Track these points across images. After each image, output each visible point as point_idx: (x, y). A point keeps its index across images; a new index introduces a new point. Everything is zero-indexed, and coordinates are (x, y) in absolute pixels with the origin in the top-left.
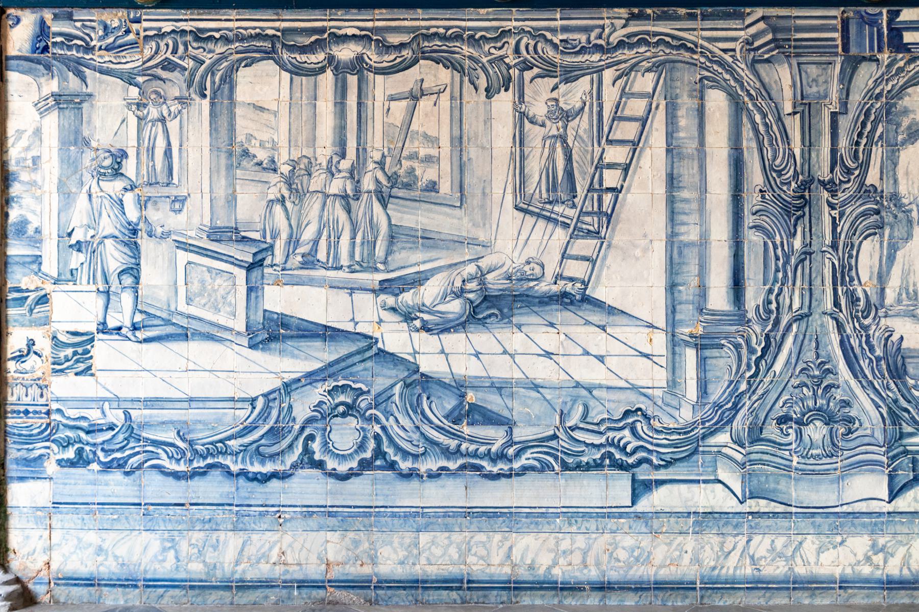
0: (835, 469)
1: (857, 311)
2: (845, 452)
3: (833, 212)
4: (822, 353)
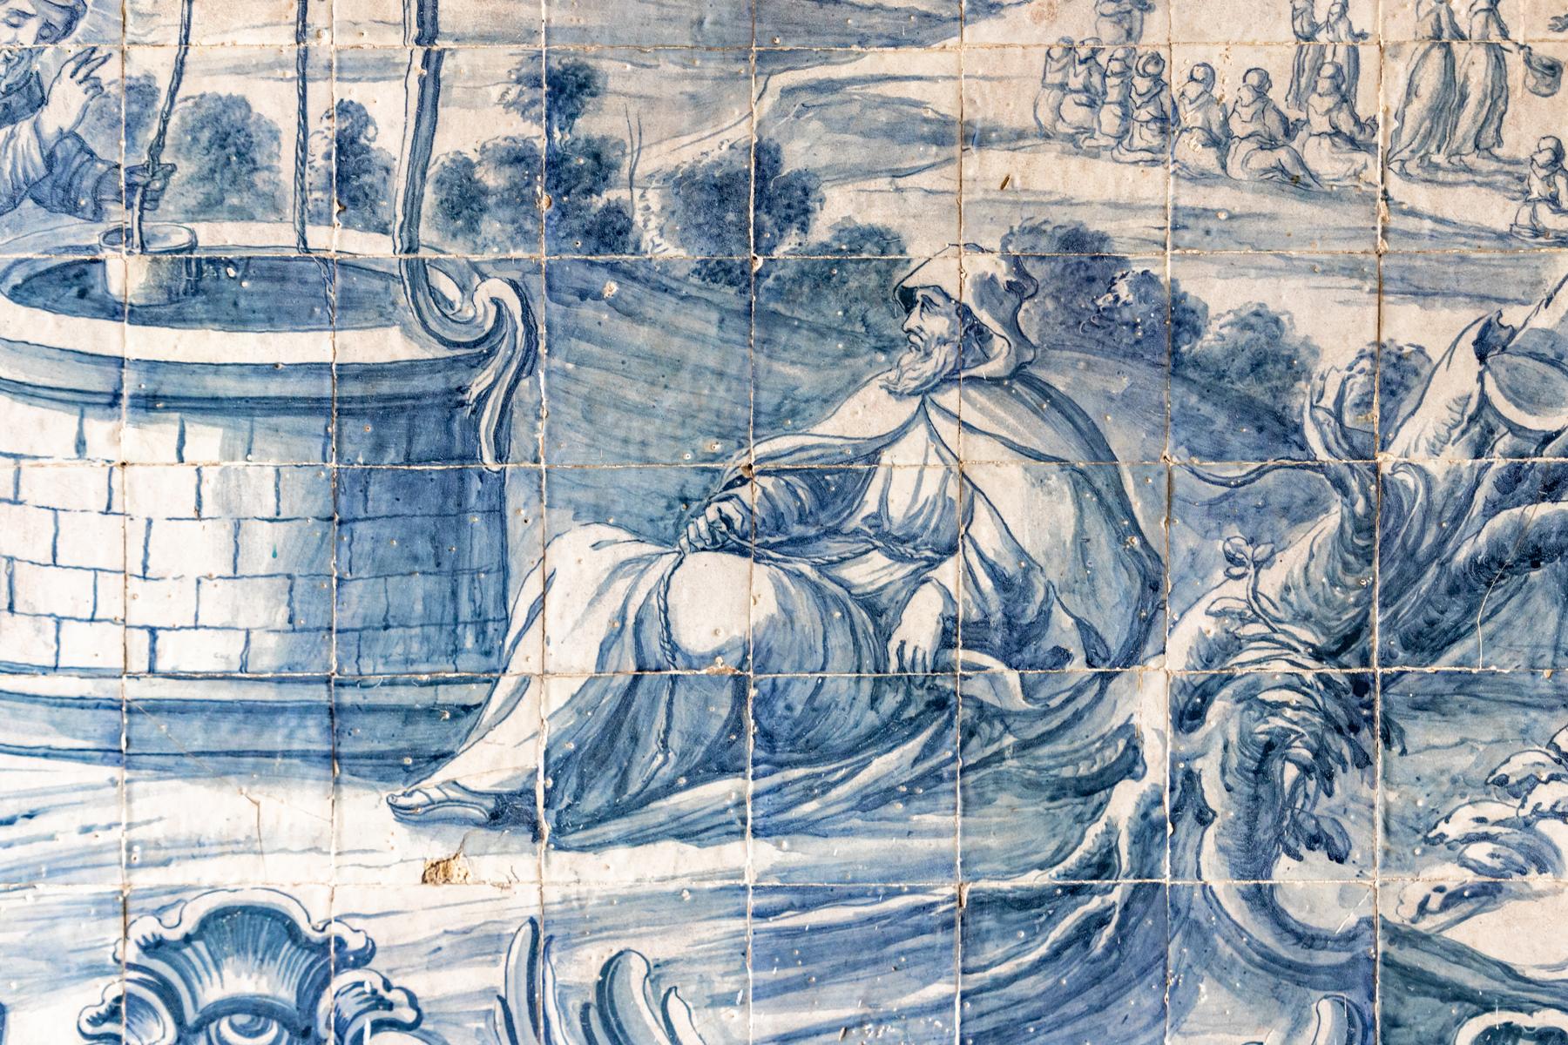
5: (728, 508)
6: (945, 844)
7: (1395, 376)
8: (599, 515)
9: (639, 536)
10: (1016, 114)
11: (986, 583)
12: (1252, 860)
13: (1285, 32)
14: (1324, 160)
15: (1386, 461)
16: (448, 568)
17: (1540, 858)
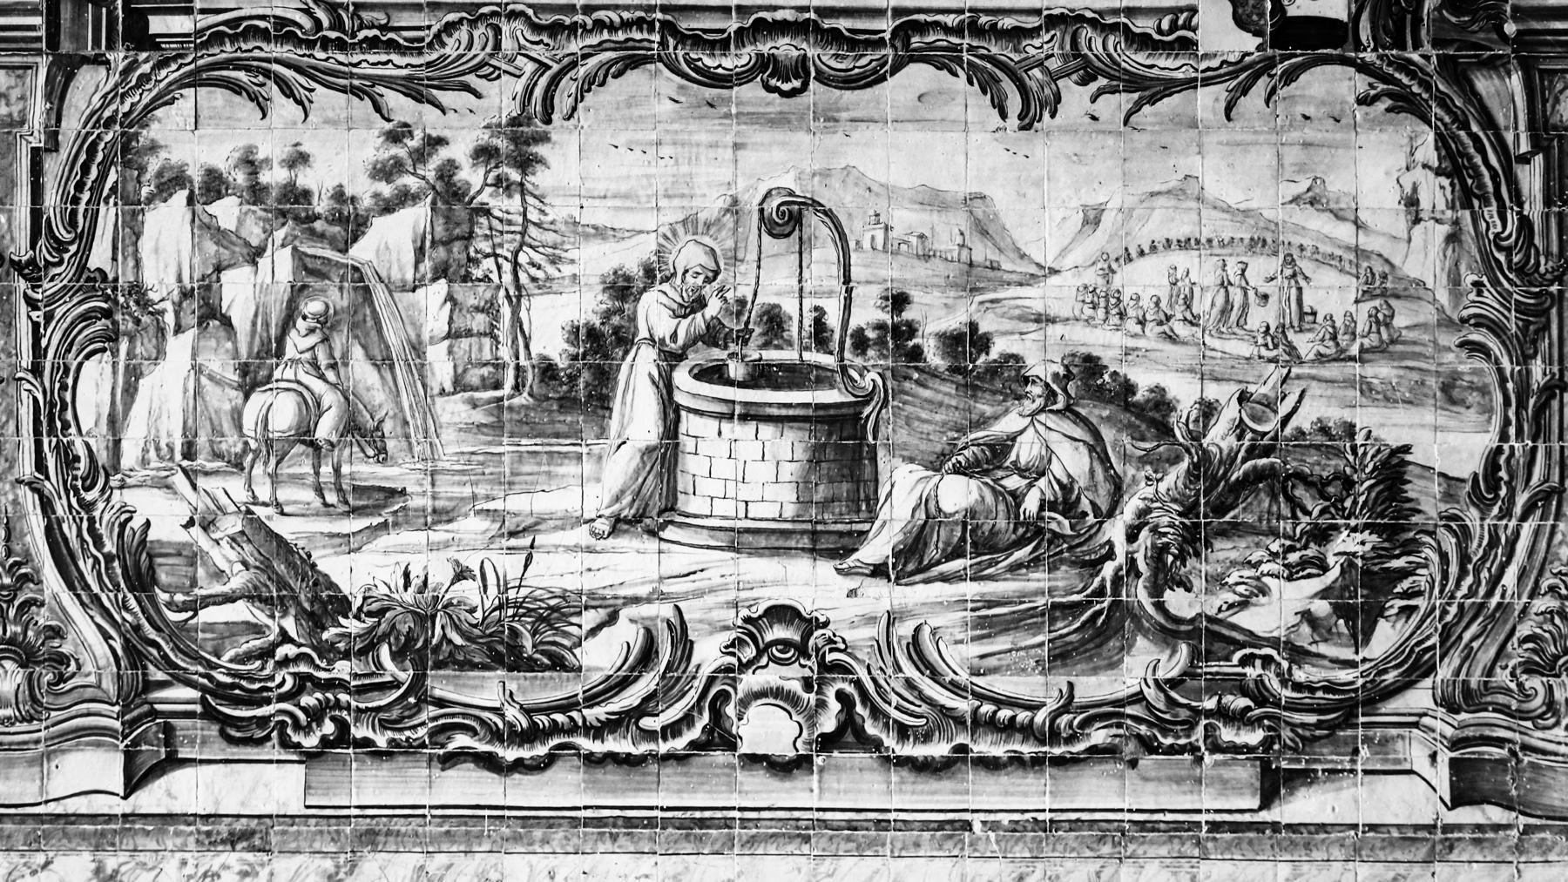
0: (37, 742)
1: (75, 478)
2: (53, 714)
3: (34, 314)
4: (18, 548)
5: (960, 458)
6: (1041, 584)
7: (1208, 410)
8: (912, 460)
9: (927, 468)
10: (1065, 312)
11: (1056, 487)
12: (1156, 591)
13: (1166, 282)
14: (1182, 330)
15: (1205, 442)
16: (857, 480)
17: (1263, 591)
